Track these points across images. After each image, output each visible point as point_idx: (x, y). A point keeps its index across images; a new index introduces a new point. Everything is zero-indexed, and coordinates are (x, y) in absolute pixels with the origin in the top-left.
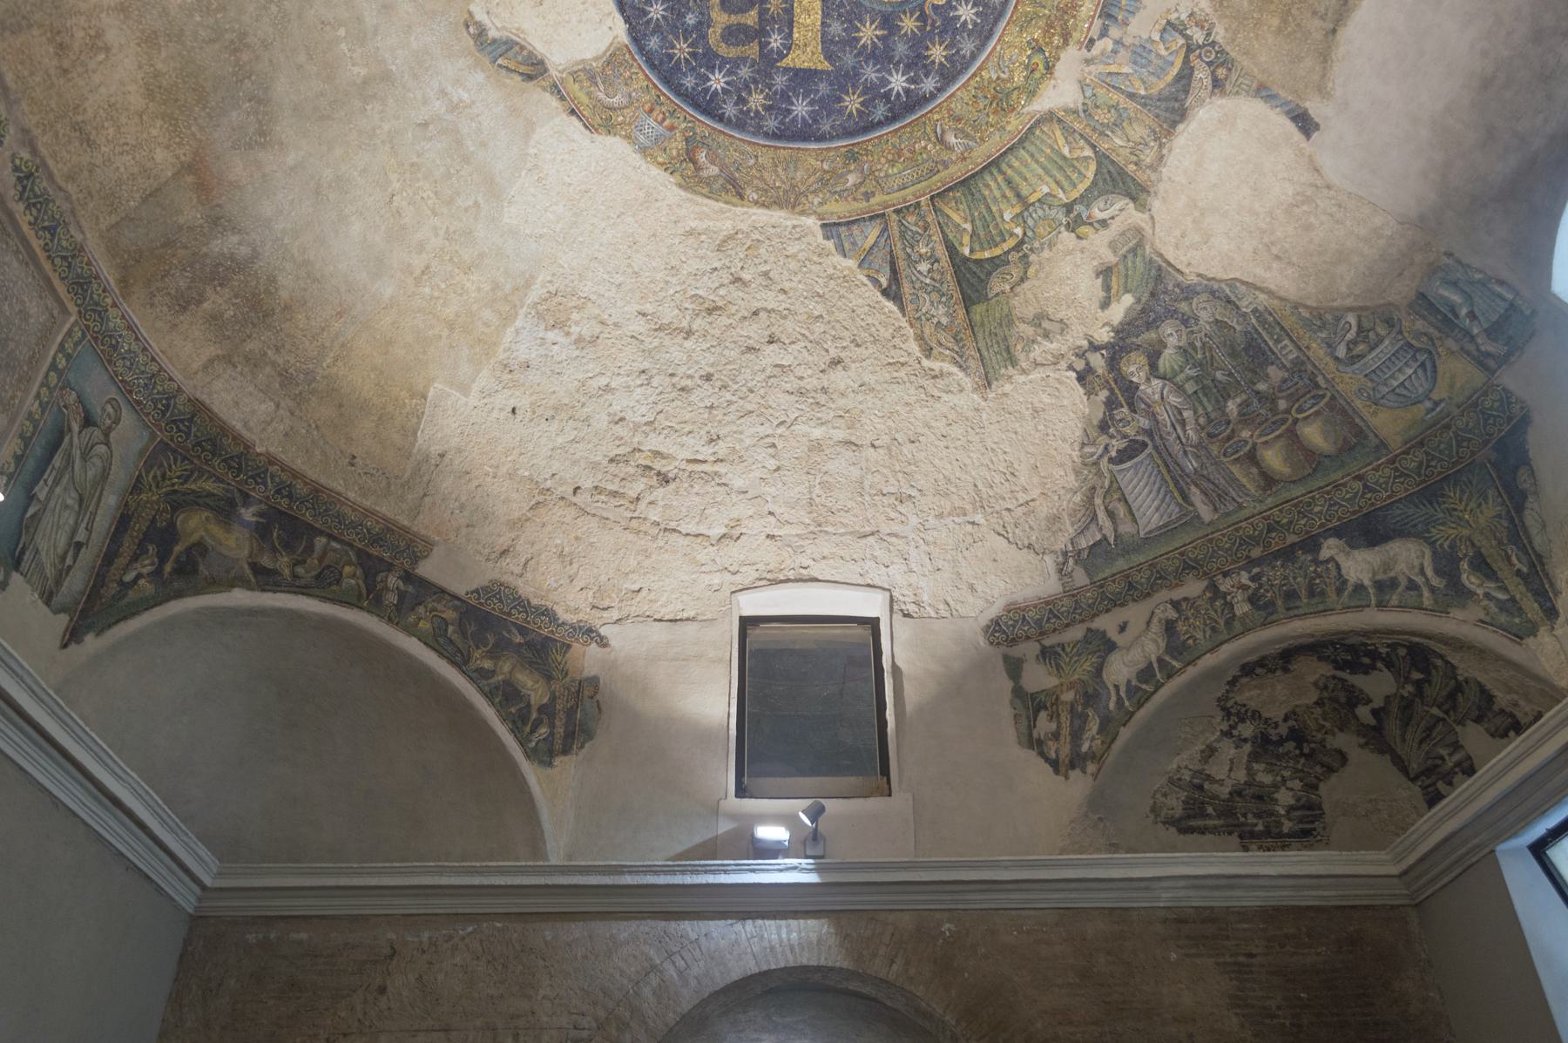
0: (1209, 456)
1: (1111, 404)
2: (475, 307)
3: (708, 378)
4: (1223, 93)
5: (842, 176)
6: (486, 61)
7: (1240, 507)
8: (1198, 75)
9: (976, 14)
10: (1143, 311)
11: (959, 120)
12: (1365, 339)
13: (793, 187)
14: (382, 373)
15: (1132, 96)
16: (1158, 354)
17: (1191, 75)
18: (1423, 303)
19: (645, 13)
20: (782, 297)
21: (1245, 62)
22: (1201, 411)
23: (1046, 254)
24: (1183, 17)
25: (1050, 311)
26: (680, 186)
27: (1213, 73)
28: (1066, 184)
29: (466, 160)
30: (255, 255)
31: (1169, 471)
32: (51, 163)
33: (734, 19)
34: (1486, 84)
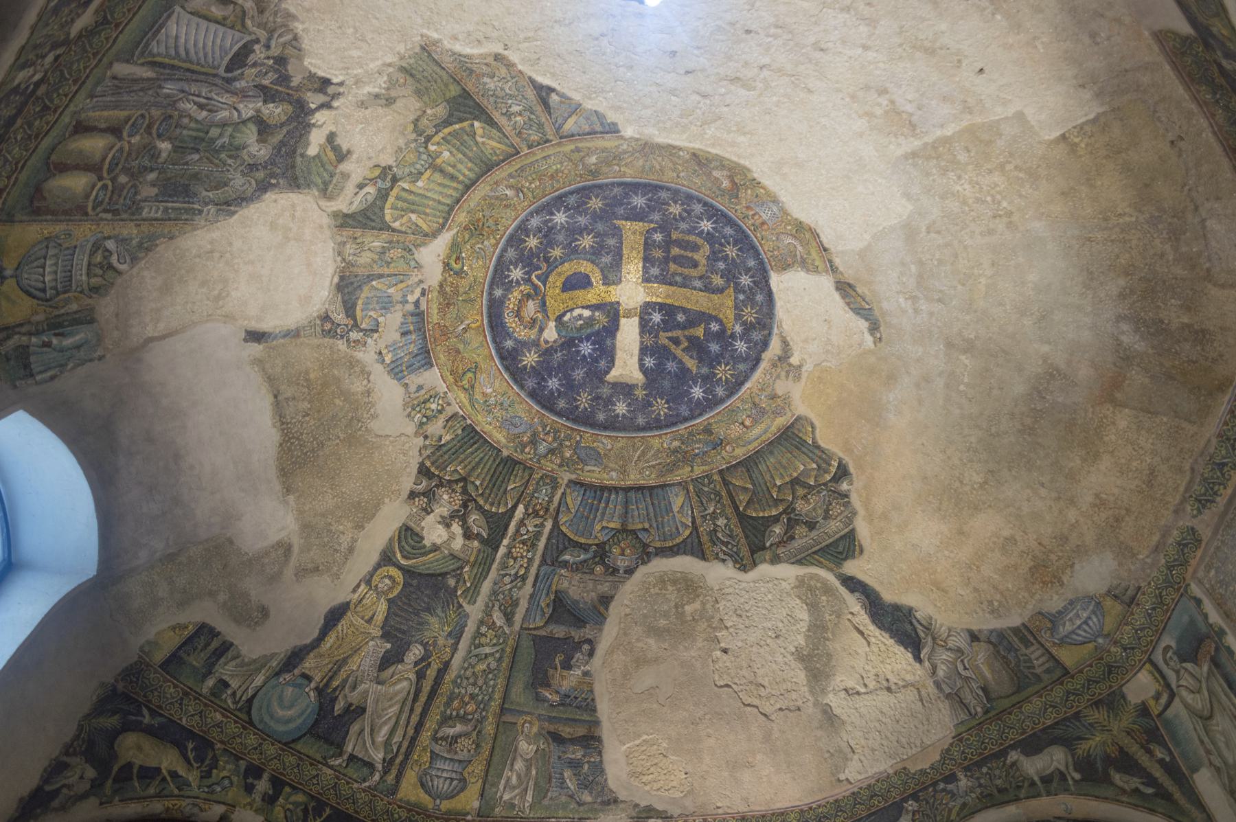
0: (156, 105)
1: (284, 79)
2: (970, 167)
3: (748, 32)
4: (320, 317)
6: (877, 312)
7: (92, 96)
8: (342, 315)
10: (294, 152)
11: (507, 206)
12: (101, 266)
14: (1088, 180)
15: (381, 276)
16: (260, 133)
17: (346, 312)
18: (87, 318)
21: (316, 341)
22: (193, 125)
23: (401, 142)
24: (369, 340)
25: (380, 110)
26: (749, 170)
28: (404, 195)
29: (921, 263)
30: (1120, 318)
31: (188, 70)
32: (1182, 489)
34: (177, 457)
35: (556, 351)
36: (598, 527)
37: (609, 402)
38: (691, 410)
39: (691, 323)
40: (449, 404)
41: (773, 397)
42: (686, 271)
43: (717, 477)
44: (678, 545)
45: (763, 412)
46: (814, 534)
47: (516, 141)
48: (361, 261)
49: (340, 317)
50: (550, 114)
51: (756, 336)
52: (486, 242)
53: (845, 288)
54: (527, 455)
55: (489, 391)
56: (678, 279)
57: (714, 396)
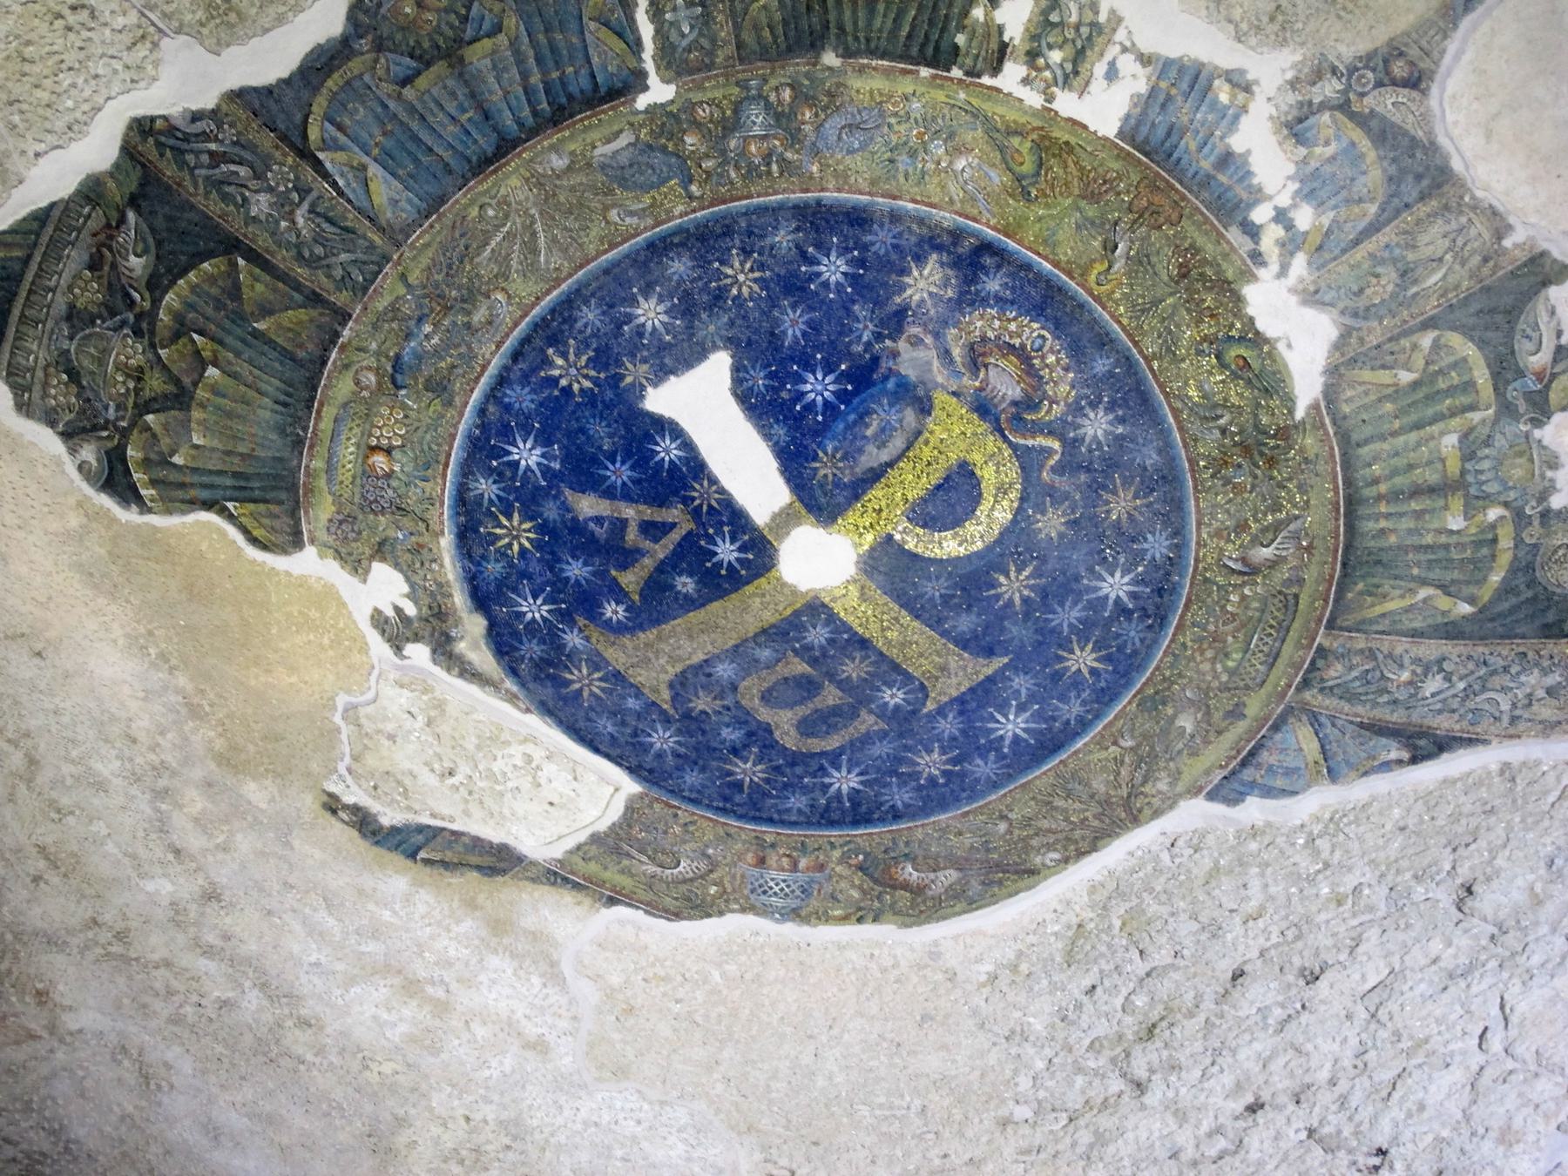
5: (1165, 732)
6: (398, 859)
9: (1108, 410)
11: (1242, 527)
13: (1106, 803)
15: (1373, 228)
19: (646, 748)
20: (1261, 923)
27: (1394, 83)
33: (803, 711)
35: (879, 337)
36: (511, 21)
37: (686, 307)
38: (507, 408)
39: (657, 586)
40: (1026, 81)
41: (382, 550)
42: (771, 679)
43: (341, 298)
44: (316, 90)
45: (371, 506)
46: (60, 303)
47: (1360, 642)
48: (1438, 228)
49: (1387, 103)
50: (1361, 725)
51: (532, 649)
52: (1217, 433)
53: (498, 861)
54: (779, 86)
55: (961, 164)
56: (765, 654)
57: (491, 470)
